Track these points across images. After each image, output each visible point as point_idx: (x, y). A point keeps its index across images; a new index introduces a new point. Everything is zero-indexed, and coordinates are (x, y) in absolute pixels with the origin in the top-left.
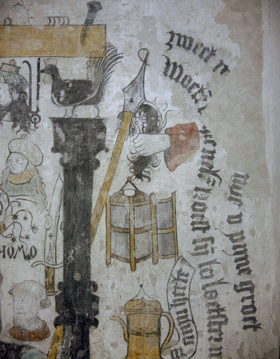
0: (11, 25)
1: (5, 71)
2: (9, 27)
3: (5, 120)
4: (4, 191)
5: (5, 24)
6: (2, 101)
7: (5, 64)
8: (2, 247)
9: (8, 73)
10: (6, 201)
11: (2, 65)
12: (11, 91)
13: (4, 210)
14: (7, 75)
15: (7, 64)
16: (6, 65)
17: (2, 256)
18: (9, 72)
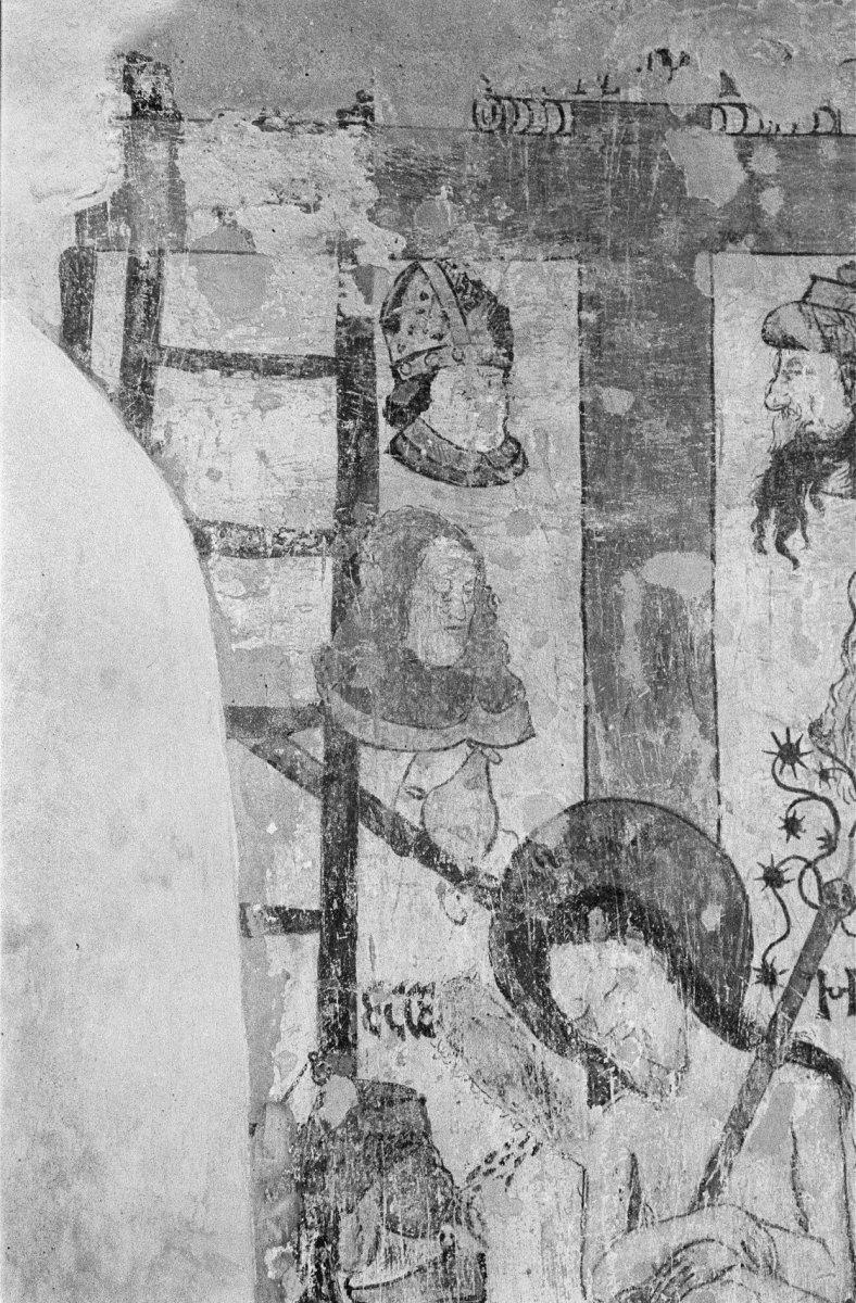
0: (840, 134)
1: (824, 307)
2: (832, 142)
3: (830, 490)
4: (841, 762)
5: (819, 130)
6: (816, 421)
7: (823, 279)
8: (844, 976)
9: (835, 313)
10: (848, 798)
11: (809, 281)
12: (848, 382)
13: (843, 835)
14: (830, 323)
15: (830, 281)
16: (825, 283)
17: (846, 1010)
18: (837, 310)
